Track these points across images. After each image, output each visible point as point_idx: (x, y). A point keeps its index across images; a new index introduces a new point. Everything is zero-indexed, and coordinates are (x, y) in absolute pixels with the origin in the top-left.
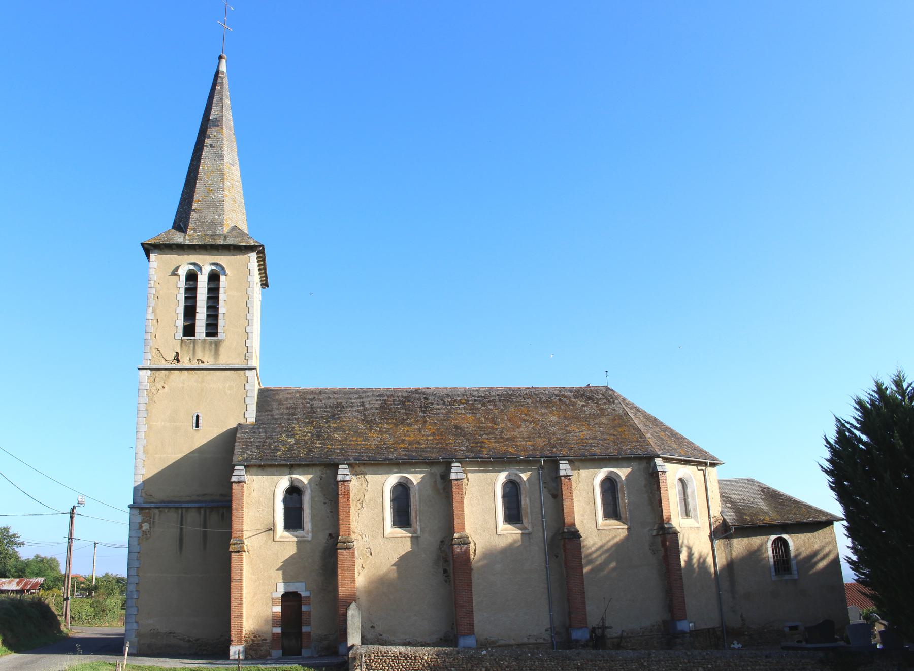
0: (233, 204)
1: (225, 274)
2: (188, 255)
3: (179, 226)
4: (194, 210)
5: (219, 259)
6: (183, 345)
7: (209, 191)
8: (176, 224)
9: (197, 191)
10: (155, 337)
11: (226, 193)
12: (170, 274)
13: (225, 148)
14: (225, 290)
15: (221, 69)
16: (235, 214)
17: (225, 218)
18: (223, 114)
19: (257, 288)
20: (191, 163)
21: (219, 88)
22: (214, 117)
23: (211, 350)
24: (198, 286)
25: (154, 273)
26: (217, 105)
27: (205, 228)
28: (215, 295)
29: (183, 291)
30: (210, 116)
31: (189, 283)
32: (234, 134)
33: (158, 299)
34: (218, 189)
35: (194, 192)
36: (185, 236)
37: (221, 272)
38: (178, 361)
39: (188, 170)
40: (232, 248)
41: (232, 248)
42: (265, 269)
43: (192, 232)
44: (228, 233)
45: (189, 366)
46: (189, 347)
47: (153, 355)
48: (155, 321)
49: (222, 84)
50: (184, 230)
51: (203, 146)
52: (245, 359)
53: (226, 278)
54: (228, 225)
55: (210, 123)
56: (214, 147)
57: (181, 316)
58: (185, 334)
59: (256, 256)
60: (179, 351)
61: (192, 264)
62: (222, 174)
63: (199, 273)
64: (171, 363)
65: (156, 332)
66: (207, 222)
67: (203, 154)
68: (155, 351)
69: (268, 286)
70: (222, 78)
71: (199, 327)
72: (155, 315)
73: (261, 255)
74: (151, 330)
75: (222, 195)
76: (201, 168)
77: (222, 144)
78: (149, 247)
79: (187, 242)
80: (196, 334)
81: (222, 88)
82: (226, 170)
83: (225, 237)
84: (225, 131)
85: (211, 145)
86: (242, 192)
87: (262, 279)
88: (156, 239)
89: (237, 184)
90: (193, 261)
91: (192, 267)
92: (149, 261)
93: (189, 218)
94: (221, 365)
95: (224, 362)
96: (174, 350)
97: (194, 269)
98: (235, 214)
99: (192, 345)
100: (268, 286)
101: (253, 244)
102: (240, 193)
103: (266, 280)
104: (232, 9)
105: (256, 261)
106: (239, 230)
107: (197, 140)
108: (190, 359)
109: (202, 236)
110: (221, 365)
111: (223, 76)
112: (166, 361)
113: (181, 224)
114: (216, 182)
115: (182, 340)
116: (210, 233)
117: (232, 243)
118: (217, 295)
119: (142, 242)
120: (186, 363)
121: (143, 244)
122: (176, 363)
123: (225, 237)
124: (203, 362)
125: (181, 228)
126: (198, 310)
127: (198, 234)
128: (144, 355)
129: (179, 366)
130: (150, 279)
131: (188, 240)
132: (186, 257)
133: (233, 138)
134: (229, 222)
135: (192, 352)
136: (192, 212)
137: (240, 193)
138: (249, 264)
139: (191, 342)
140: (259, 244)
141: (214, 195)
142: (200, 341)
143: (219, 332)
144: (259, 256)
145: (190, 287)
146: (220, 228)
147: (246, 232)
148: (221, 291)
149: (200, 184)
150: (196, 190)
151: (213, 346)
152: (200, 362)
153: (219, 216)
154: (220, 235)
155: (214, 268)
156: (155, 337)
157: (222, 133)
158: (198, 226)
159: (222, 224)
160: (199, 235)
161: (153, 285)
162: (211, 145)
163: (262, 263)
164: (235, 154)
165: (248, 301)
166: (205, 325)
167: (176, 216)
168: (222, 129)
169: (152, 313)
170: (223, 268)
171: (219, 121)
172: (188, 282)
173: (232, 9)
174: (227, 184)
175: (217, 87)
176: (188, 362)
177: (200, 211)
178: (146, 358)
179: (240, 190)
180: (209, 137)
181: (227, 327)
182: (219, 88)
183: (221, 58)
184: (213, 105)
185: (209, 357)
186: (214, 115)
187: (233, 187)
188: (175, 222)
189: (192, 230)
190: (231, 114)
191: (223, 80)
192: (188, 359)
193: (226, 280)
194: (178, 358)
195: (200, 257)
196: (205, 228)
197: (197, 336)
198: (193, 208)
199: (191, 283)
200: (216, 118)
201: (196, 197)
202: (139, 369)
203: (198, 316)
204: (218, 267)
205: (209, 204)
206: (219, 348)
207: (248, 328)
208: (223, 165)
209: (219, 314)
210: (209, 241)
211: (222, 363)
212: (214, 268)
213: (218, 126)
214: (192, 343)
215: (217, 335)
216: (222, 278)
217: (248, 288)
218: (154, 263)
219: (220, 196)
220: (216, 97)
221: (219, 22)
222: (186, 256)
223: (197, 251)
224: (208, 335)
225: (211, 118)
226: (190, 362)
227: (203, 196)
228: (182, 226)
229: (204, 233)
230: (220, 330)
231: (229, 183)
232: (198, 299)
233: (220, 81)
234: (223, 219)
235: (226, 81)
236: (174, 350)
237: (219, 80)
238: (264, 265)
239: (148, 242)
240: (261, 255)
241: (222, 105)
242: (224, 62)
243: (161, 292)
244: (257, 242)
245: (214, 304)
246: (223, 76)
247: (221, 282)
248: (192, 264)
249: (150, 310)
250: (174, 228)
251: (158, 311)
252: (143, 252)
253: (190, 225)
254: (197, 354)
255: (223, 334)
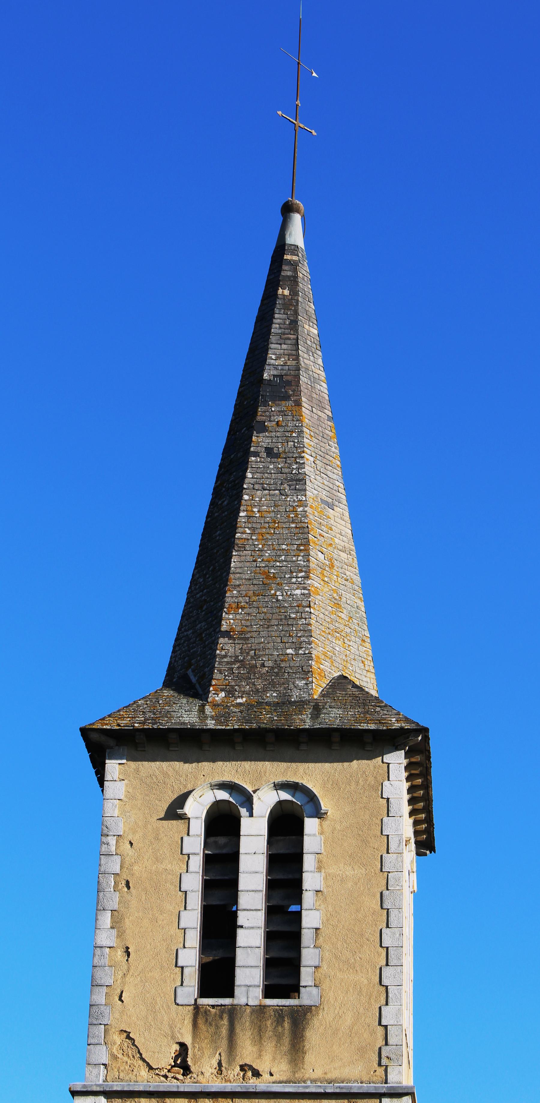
0: (332, 613)
1: (318, 813)
2: (214, 761)
3: (185, 678)
4: (227, 634)
5: (301, 770)
6: (200, 1021)
7: (268, 577)
8: (176, 675)
9: (233, 579)
10: (120, 999)
11: (314, 582)
12: (162, 815)
13: (308, 458)
14: (319, 861)
15: (290, 240)
16: (340, 643)
17: (314, 653)
18: (298, 362)
19: (410, 853)
20: (213, 504)
21: (286, 292)
22: (275, 373)
23: (279, 1037)
24: (242, 851)
25: (116, 813)
26: (282, 339)
27: (260, 684)
28: (290, 876)
29: (197, 863)
30: (263, 370)
31: (216, 842)
32: (329, 419)
33: (128, 887)
34: (292, 572)
35: (225, 582)
36: (203, 706)
37: (308, 808)
38: (186, 1070)
39: (206, 523)
40: (336, 738)
41: (336, 738)
42: (428, 799)
43: (223, 694)
44: (323, 695)
45: (217, 1085)
46: (217, 1027)
47: (115, 1051)
48: (120, 953)
49: (293, 282)
50: (201, 692)
51: (247, 453)
52: (380, 1064)
53: (321, 825)
54: (322, 674)
55: (265, 391)
56: (277, 456)
57: (194, 939)
58: (205, 991)
59: (405, 762)
60: (188, 1040)
61: (223, 786)
62: (303, 530)
63: (243, 811)
64: (166, 1077)
65: (123, 983)
66: (263, 665)
67: (249, 475)
68: (118, 1039)
69: (432, 849)
70: (294, 266)
71: (247, 970)
72: (120, 935)
73: (417, 759)
74: (106, 977)
75: (305, 588)
76: (242, 514)
77: (300, 447)
78: (103, 739)
79: (211, 724)
80: (237, 991)
81: (294, 292)
82: (313, 516)
83: (317, 709)
84: (305, 411)
85: (269, 451)
86: (357, 579)
87: (418, 827)
88: (122, 718)
89: (344, 555)
90: (227, 778)
91: (223, 795)
92: (101, 781)
93: (215, 656)
94: (309, 1083)
95: (318, 1073)
96: (173, 1037)
97: (292, 802)
98: (340, 643)
99: (225, 1022)
100: (432, 849)
101: (397, 726)
102: (353, 583)
103: (430, 831)
104: (314, 74)
105: (404, 775)
106: (355, 686)
107: (228, 440)
108: (220, 1064)
109: (249, 706)
110: (309, 1083)
111: (295, 258)
112: (151, 1068)
113: (190, 672)
114: (287, 553)
115: (196, 1007)
116: (272, 696)
117: (337, 724)
118: (297, 876)
119: (83, 725)
120: (207, 1074)
121: (85, 732)
122: (180, 1077)
123: (317, 709)
124: (256, 1074)
125: (192, 686)
126: (242, 918)
127: (239, 700)
128: (89, 1051)
129: (188, 1085)
130: (105, 831)
131: (212, 717)
132: (206, 766)
133: (329, 429)
134: (326, 666)
135: (224, 1043)
136: (221, 640)
137: (353, 583)
138: (386, 783)
139: (222, 1012)
140: (413, 726)
141: (282, 590)
142: (248, 1010)
143: (302, 984)
144: (413, 760)
145: (217, 852)
146: (301, 683)
147: (374, 693)
148: (309, 862)
149: (243, 558)
150: (231, 576)
151: (287, 1025)
152: (250, 1074)
153: (297, 649)
154: (301, 704)
155: (285, 796)
156: (120, 999)
157: (298, 417)
158: (240, 678)
159: (306, 673)
160: (240, 704)
161: (113, 849)
162: (269, 451)
163: (419, 781)
164: (336, 475)
165: (386, 893)
166: (261, 963)
167: (173, 652)
168: (298, 404)
169: (112, 928)
170: (312, 798)
171: (289, 383)
172: (212, 839)
173: (314, 74)
174: (317, 557)
175: (280, 291)
176: (215, 1072)
177: (243, 637)
178: (93, 1061)
179: (353, 573)
180: (263, 429)
181: (325, 966)
182: (286, 292)
183: (288, 209)
184: (273, 339)
185: (274, 1059)
186: (275, 367)
187: (332, 566)
188: (171, 669)
189: (222, 690)
190: (320, 361)
191: (295, 271)
192: (215, 1063)
193: (322, 833)
194: (185, 1061)
195: (247, 765)
196: (260, 684)
197: (240, 997)
198: (224, 627)
199: (222, 840)
200: (281, 376)
201: (231, 596)
202: (74, 1093)
203: (242, 938)
204: (298, 794)
205: (269, 616)
206: (304, 1029)
207: (387, 972)
208: (302, 504)
209: (304, 932)
210: (271, 720)
211: (314, 1076)
212: (285, 796)
213: (286, 397)
214: (226, 1016)
215: (298, 991)
216: (311, 825)
217: (385, 855)
218: (119, 784)
219: (298, 592)
220: (279, 318)
221: (280, 113)
222: (205, 764)
223: (238, 748)
224: (269, 992)
225: (266, 376)
226: (220, 1071)
227: (251, 593)
228: (194, 680)
229: (254, 698)
230: (306, 977)
231: (321, 556)
232: (241, 886)
233: (289, 273)
234: (309, 657)
235: (304, 271)
236: (173, 1037)
237: (286, 272)
238: (427, 786)
239: (98, 726)
240: (417, 759)
241: (297, 339)
242: (297, 219)
243: (136, 868)
244: (407, 720)
245: (281, 903)
246: (295, 258)
247: (306, 839)
248: (223, 786)
249: (106, 919)
250: (168, 684)
251: (127, 923)
252: (86, 755)
253: (216, 675)
254: (239, 1050)
255: (314, 989)
